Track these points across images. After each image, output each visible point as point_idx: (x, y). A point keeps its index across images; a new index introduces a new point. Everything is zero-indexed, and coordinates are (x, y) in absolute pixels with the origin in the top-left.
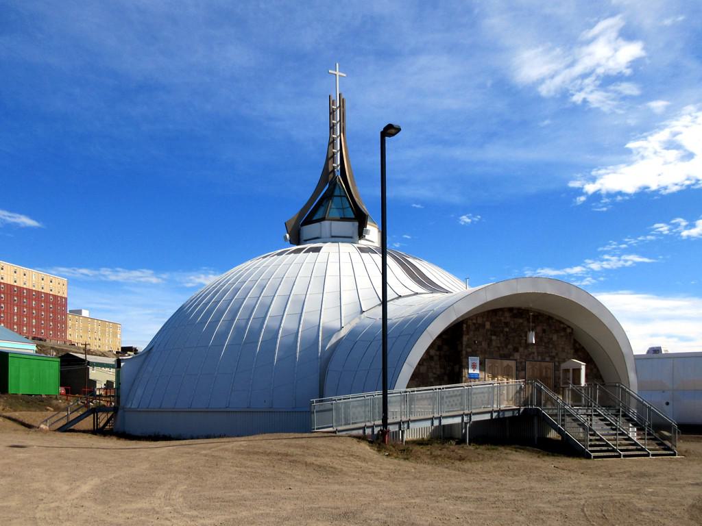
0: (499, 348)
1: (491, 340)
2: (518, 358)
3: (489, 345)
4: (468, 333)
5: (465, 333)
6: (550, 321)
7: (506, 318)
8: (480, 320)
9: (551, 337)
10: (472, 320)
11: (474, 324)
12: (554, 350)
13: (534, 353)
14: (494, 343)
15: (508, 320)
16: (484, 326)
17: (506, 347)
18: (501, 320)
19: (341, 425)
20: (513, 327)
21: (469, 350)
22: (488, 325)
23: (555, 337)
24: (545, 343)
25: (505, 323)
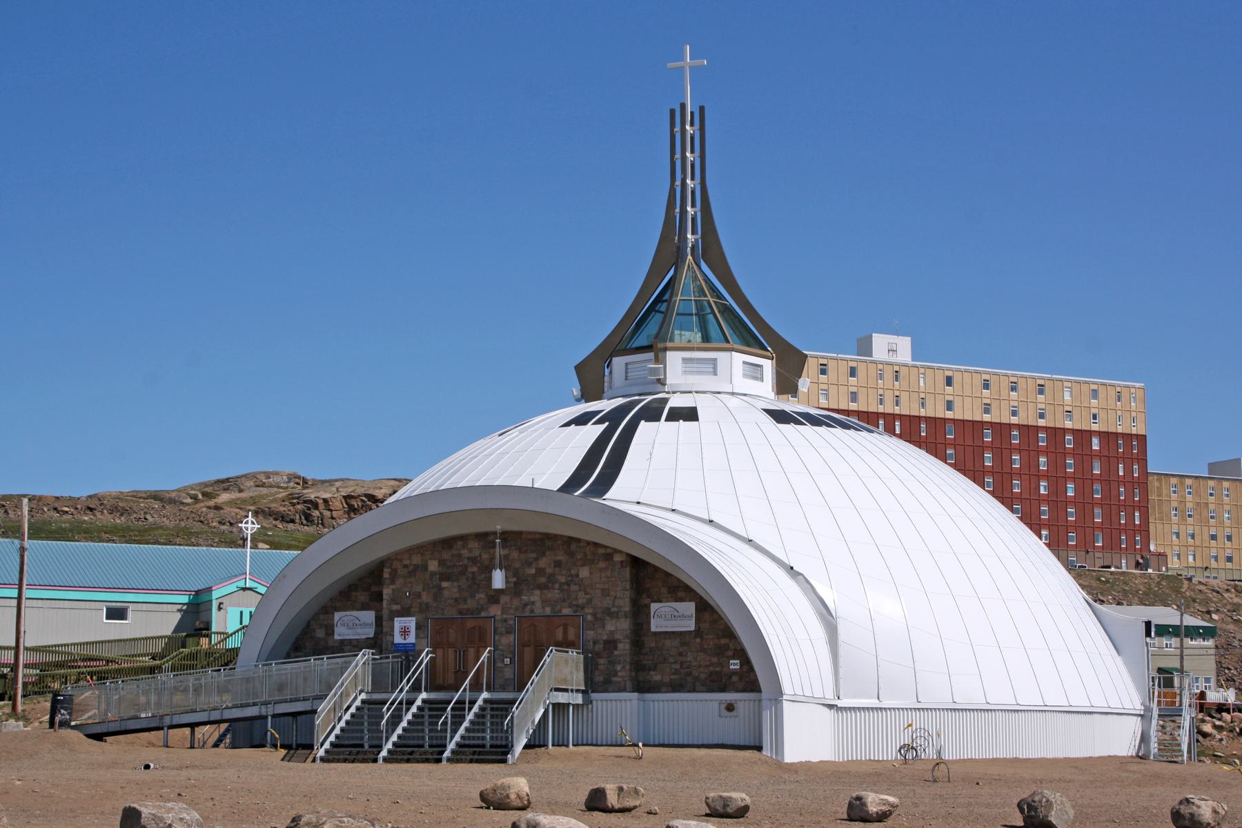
0: (456, 600)
1: (440, 589)
2: (499, 613)
3: (436, 597)
4: (393, 582)
5: (387, 581)
6: (573, 547)
7: (471, 550)
8: (417, 560)
9: (573, 572)
10: (401, 560)
11: (406, 566)
12: (581, 594)
13: (533, 603)
14: (446, 593)
15: (476, 553)
16: (425, 567)
17: (473, 596)
18: (460, 555)
19: (446, 737)
20: (469, 570)
21: (395, 607)
22: (433, 566)
23: (584, 572)
24: (562, 584)
25: (469, 559)
